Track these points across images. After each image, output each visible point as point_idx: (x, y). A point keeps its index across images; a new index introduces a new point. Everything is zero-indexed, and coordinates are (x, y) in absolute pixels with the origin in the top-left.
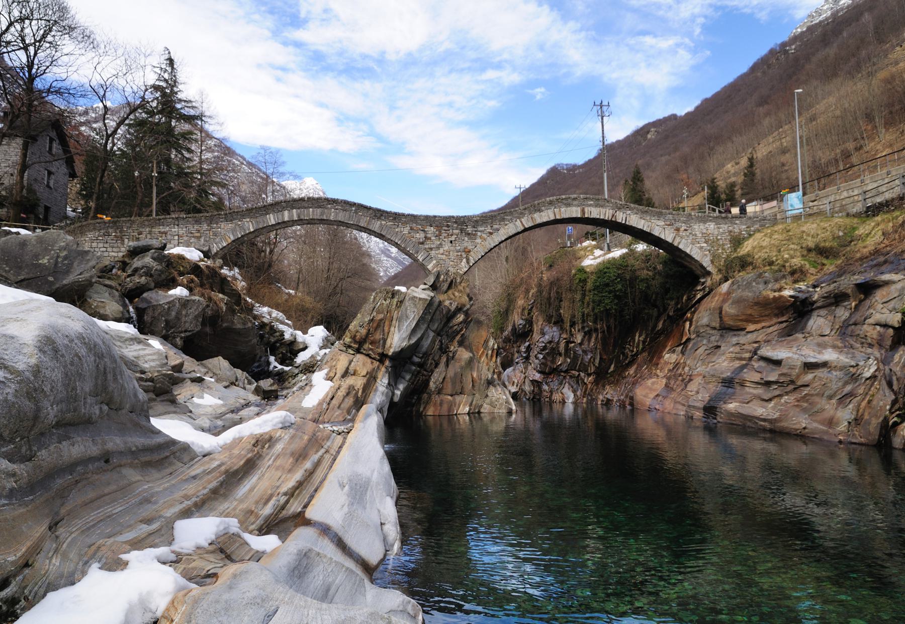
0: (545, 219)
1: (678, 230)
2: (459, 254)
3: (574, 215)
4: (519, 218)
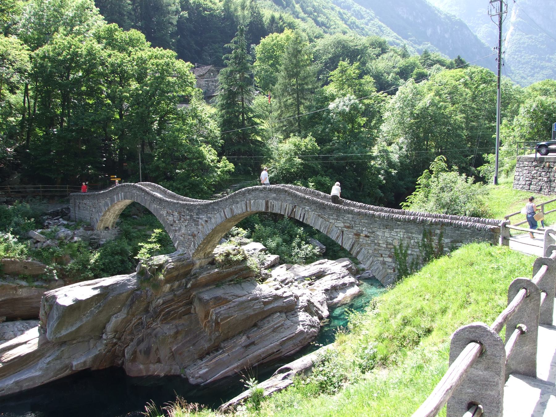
1: (358, 235)
2: (190, 237)
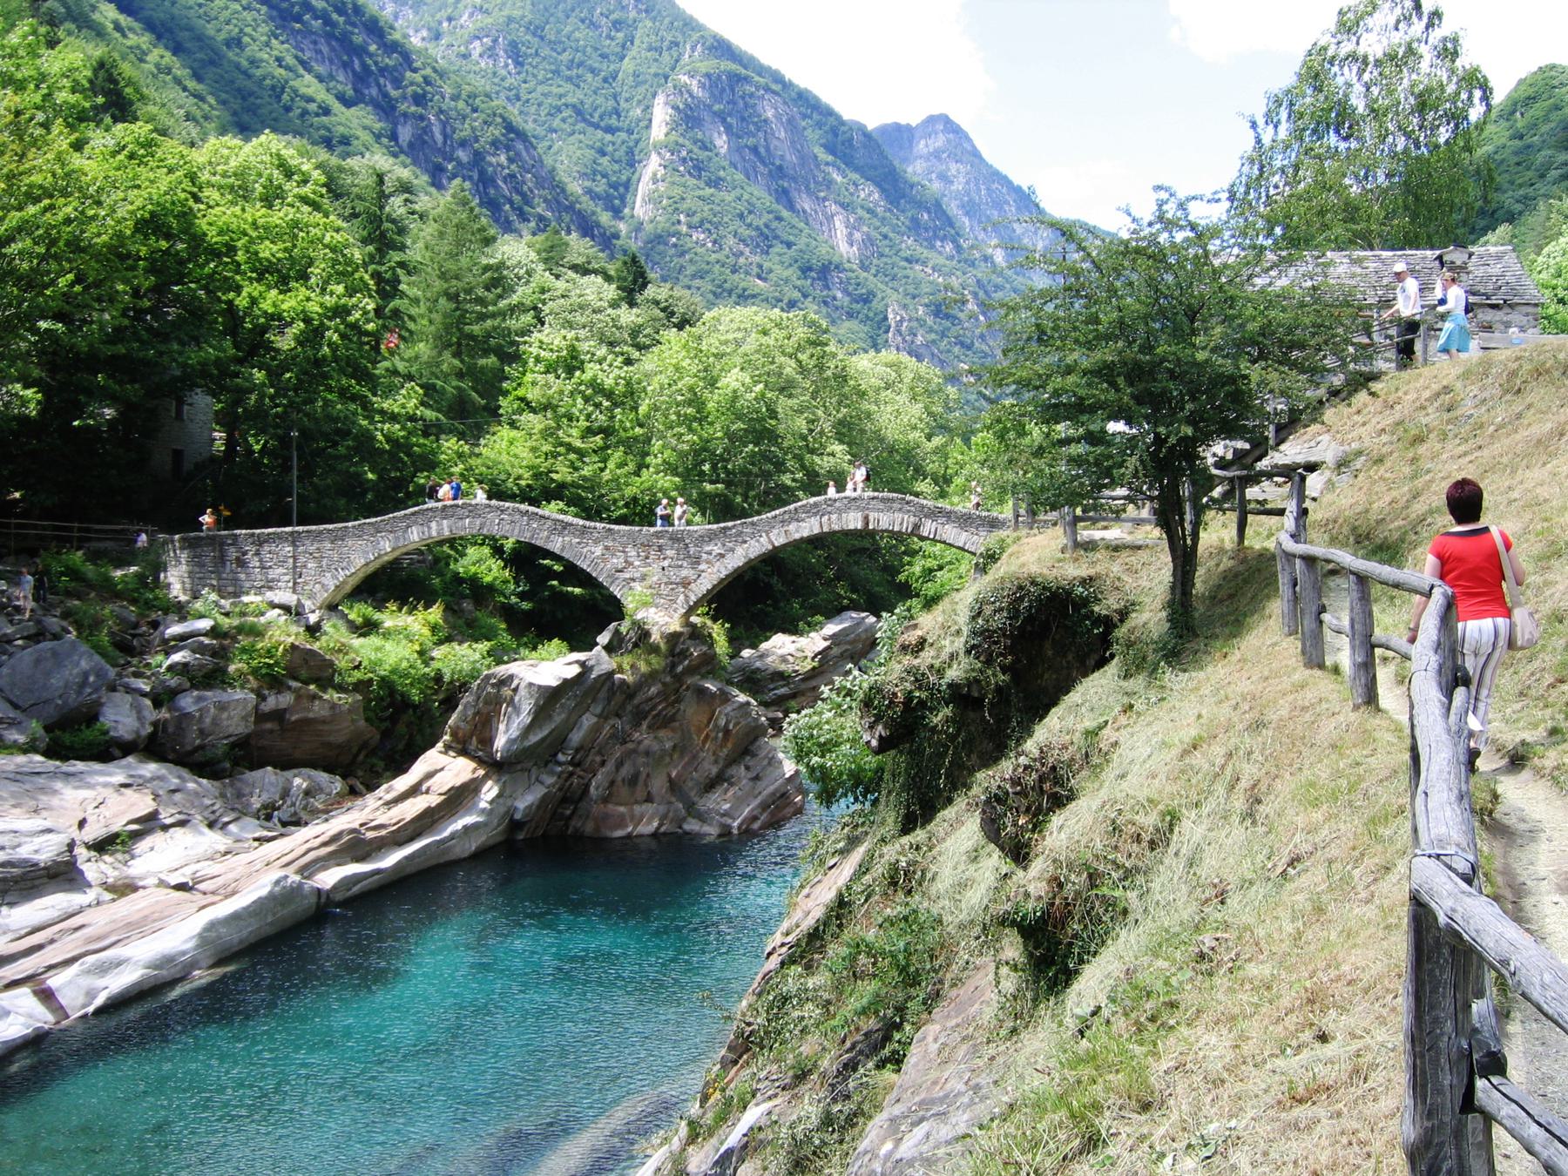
0: (805, 534)
3: (851, 527)
4: (767, 533)
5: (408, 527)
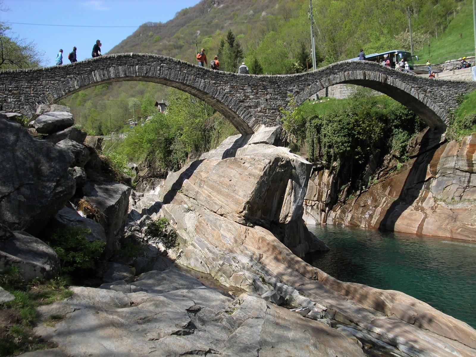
3: (359, 78)
4: (319, 79)
5: (91, 71)
